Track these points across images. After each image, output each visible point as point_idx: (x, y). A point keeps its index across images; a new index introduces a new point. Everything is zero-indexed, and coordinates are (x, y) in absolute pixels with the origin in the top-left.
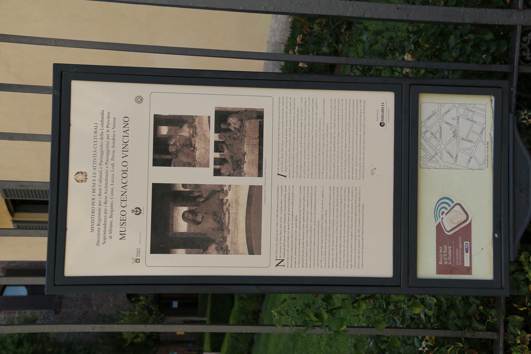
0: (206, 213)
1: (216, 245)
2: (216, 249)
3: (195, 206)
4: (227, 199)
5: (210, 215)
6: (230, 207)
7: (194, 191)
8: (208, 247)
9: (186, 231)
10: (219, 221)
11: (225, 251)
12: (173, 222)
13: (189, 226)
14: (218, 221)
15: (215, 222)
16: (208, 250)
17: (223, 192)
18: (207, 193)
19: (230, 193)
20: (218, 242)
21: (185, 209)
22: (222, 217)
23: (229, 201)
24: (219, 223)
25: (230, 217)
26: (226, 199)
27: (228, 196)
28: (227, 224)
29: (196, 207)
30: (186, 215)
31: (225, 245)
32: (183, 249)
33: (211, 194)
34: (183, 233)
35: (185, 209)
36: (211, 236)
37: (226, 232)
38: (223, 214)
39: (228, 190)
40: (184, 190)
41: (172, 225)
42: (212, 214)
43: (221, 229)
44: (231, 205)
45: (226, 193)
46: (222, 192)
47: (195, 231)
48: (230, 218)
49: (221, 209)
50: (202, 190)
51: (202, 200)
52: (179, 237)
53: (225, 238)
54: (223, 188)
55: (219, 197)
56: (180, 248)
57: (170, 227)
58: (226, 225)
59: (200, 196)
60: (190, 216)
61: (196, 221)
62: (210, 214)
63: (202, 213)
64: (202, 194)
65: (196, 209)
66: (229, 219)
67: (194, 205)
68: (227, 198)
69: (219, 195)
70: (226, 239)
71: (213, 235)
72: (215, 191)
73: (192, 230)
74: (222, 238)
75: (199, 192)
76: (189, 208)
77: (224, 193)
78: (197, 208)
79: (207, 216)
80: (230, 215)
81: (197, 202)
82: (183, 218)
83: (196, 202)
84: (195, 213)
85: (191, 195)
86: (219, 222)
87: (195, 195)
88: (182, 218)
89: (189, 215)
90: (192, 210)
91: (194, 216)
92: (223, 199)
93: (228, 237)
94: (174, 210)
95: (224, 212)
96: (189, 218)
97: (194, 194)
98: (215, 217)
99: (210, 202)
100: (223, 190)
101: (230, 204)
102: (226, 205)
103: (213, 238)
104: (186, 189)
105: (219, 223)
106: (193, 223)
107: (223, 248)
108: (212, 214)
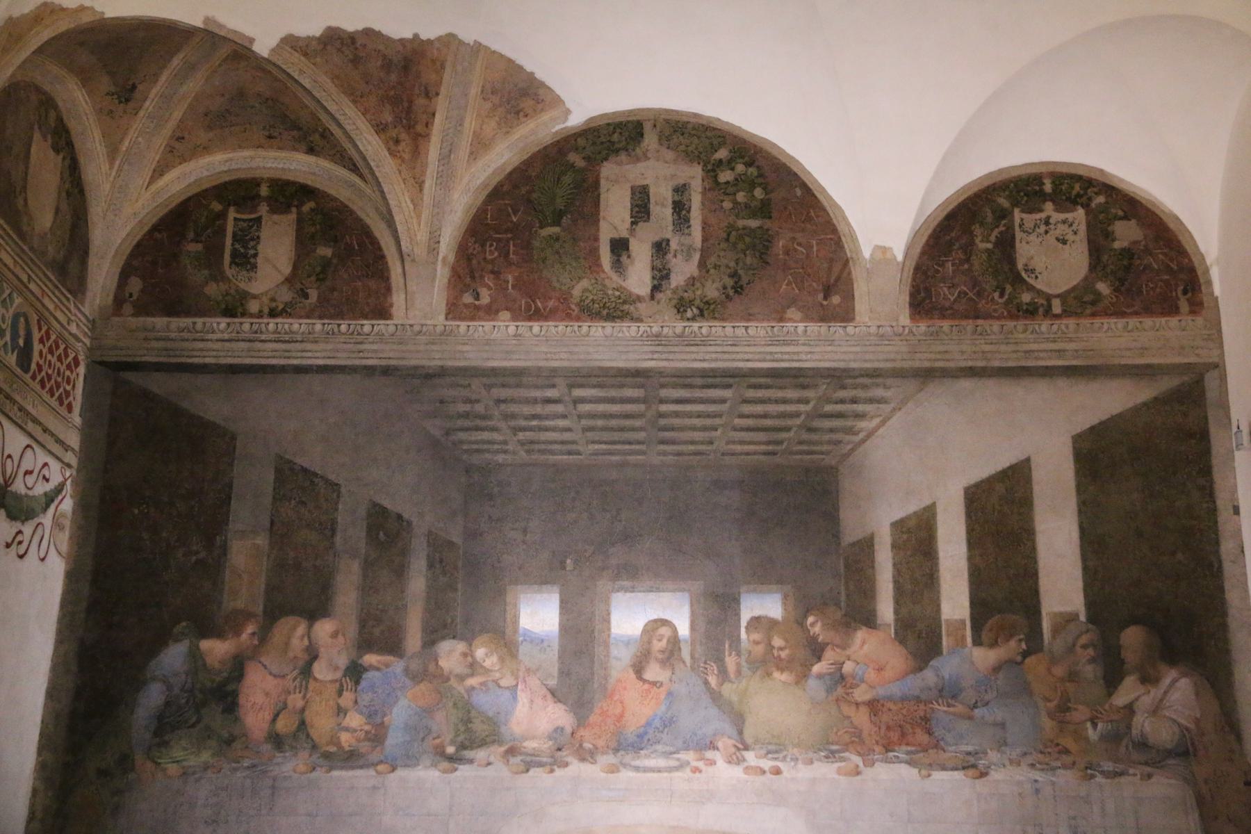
0: (670, 694)
1: (569, 730)
2: (556, 730)
3: (692, 657)
4: (715, 764)
5: (663, 708)
6: (691, 774)
7: (739, 654)
8: (564, 704)
9: (613, 630)
10: (646, 738)
11: (552, 757)
12: (640, 591)
13: (628, 642)
14: (646, 733)
15: (643, 721)
16: (555, 702)
17: (739, 749)
18: (735, 698)
19: (737, 772)
20: (578, 736)
21: (684, 630)
22: (659, 747)
23: (710, 769)
24: (638, 736)
25: (659, 771)
26: (715, 758)
27: (726, 765)
28: (637, 763)
29: (688, 665)
30: (665, 631)
31: (569, 759)
32: (560, 625)
33: (733, 708)
34: (607, 620)
35: (684, 630)
36: (597, 710)
37: (610, 759)
38: (669, 749)
39: (746, 764)
40: (744, 623)
41: (632, 589)
42: (669, 713)
43: (619, 744)
44: (697, 775)
45: (738, 758)
46: (740, 746)
47: (613, 663)
48: (654, 771)
49: (684, 743)
50: (744, 682)
51: (713, 681)
52: (597, 612)
53: (592, 758)
54: (753, 749)
55: (723, 735)
56: (560, 614)
57: (626, 583)
58: (633, 759)
59: (723, 674)
60: (658, 645)
61: (644, 664)
62: (669, 708)
63: (671, 681)
64: (730, 681)
65: (684, 662)
66: (652, 770)
67: (697, 656)
68: (721, 763)
69: (729, 737)
70: (587, 760)
71: (601, 718)
72: (743, 723)
73: (616, 652)
74: (591, 746)
75: (739, 672)
76: (686, 641)
77: (738, 753)
78: (686, 666)
79: (663, 697)
80: (666, 774)
81: (707, 666)
82: (655, 621)
83: (705, 663)
84: (669, 658)
85: (727, 646)
86: (643, 737)
87: (727, 659)
88: (656, 617)
89: (665, 641)
90: (680, 649)
91: (660, 656)
92: (715, 748)
93: (592, 765)
94: (679, 594)
95: (674, 753)
96: (655, 642)
97: (730, 655)
98: (657, 723)
99: (706, 708)
100: (746, 748)
101: (700, 772)
102: (698, 760)
103: (593, 718)
104: (747, 628)
105: (640, 736)
106: (639, 654)
107: (559, 753)
108: (669, 713)
